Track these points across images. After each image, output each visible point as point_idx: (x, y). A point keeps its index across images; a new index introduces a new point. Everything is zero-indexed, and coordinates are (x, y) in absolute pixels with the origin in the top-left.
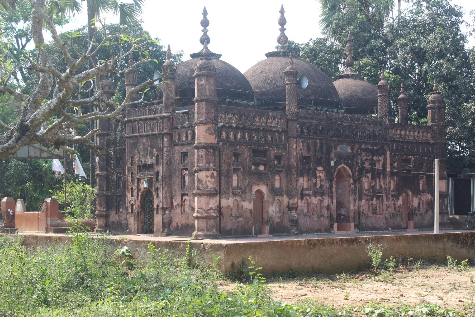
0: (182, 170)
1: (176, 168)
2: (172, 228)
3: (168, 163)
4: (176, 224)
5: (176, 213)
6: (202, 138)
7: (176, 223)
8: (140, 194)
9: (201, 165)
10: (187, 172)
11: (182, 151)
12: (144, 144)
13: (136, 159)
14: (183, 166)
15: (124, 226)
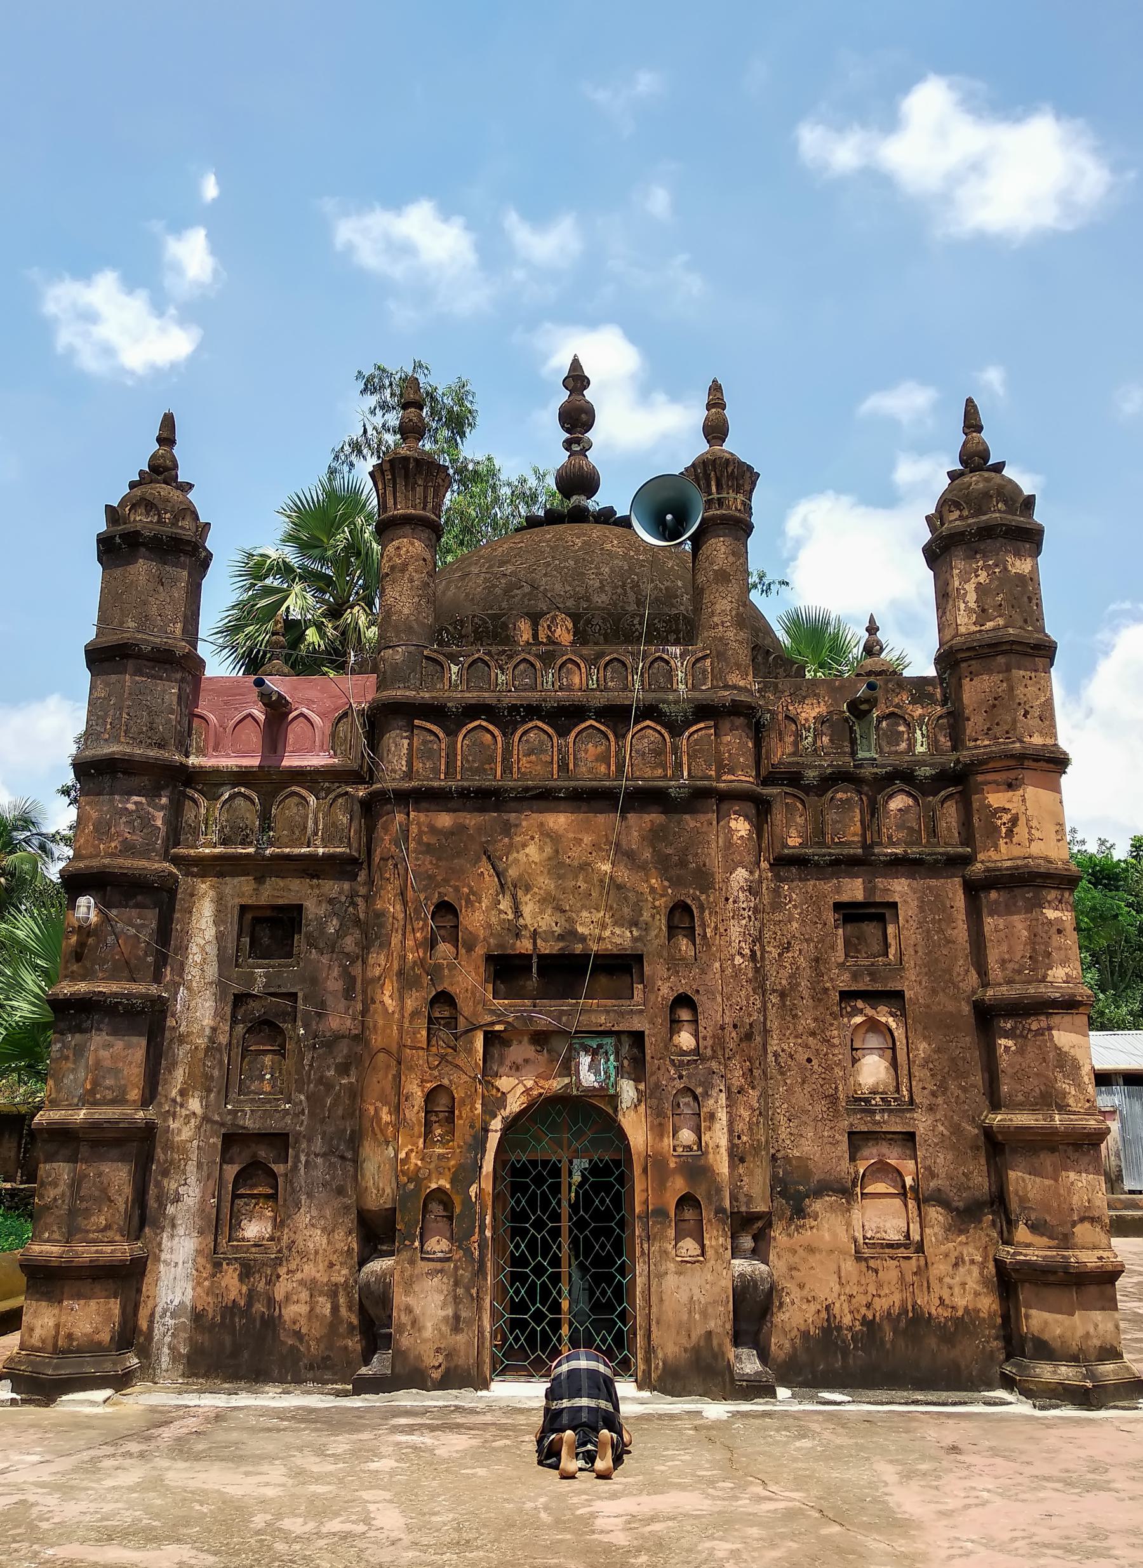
0: (847, 996)
1: (794, 986)
2: (780, 1344)
3: (758, 953)
4: (810, 1317)
5: (811, 1250)
6: (1054, 837)
7: (813, 1307)
8: (496, 1124)
9: (1058, 974)
10: (883, 1009)
11: (845, 898)
12: (553, 837)
13: (475, 920)
14: (855, 976)
15: (298, 1335)
